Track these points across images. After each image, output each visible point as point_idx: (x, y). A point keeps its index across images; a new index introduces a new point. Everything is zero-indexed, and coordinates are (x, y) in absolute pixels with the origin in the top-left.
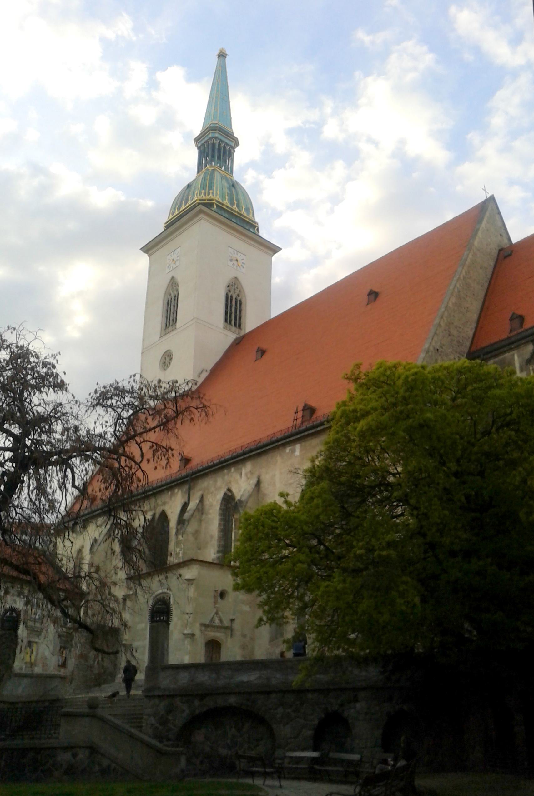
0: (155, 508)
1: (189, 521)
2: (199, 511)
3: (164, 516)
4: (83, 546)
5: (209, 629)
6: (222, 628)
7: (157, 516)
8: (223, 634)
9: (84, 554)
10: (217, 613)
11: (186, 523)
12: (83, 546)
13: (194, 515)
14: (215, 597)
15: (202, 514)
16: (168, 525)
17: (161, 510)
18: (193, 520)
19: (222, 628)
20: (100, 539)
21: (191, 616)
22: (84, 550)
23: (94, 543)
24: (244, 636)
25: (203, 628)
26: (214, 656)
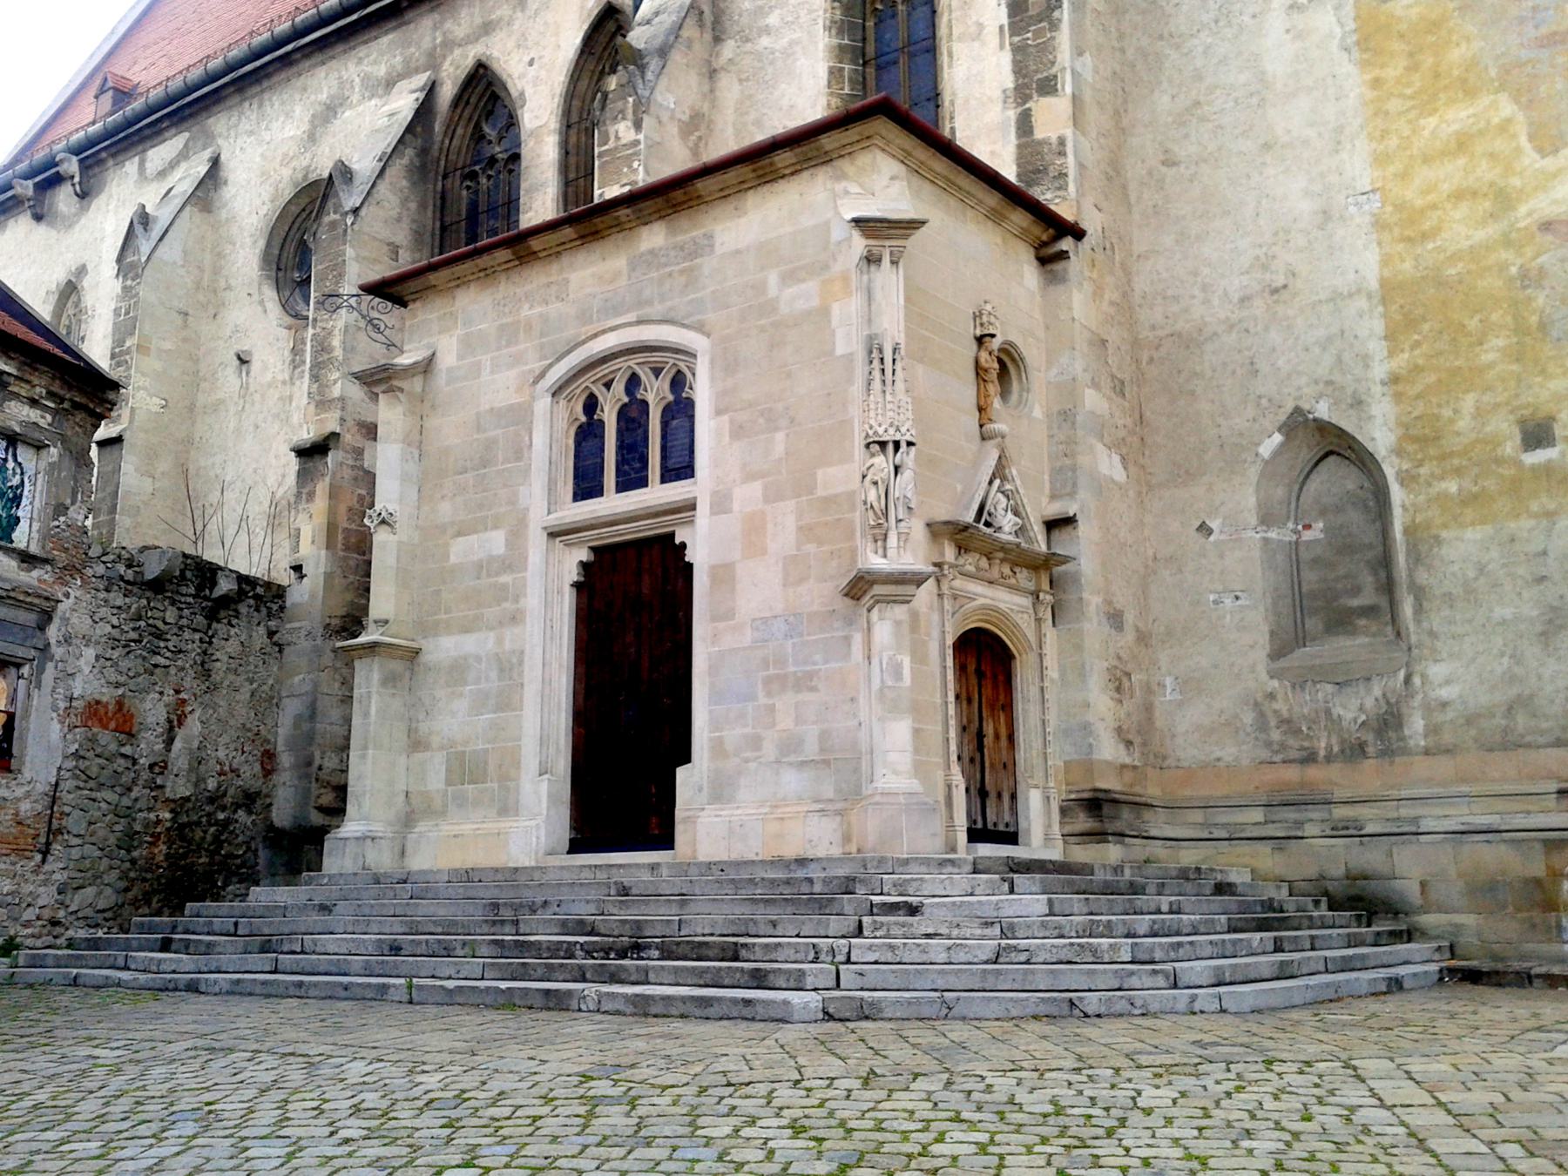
0: (433, 62)
1: (663, 52)
2: (701, 23)
3: (484, 93)
4: (82, 270)
5: (970, 562)
6: (1019, 559)
7: (447, 92)
8: (1026, 602)
9: (88, 300)
10: (999, 472)
11: (654, 64)
12: (82, 270)
13: (685, 33)
14: (979, 370)
15: (717, 40)
16: (512, 122)
17: (469, 63)
18: (676, 57)
19: (1019, 559)
20: (163, 216)
21: (907, 457)
22: (86, 283)
23: (139, 229)
24: (1115, 619)
25: (949, 553)
26: (989, 729)
